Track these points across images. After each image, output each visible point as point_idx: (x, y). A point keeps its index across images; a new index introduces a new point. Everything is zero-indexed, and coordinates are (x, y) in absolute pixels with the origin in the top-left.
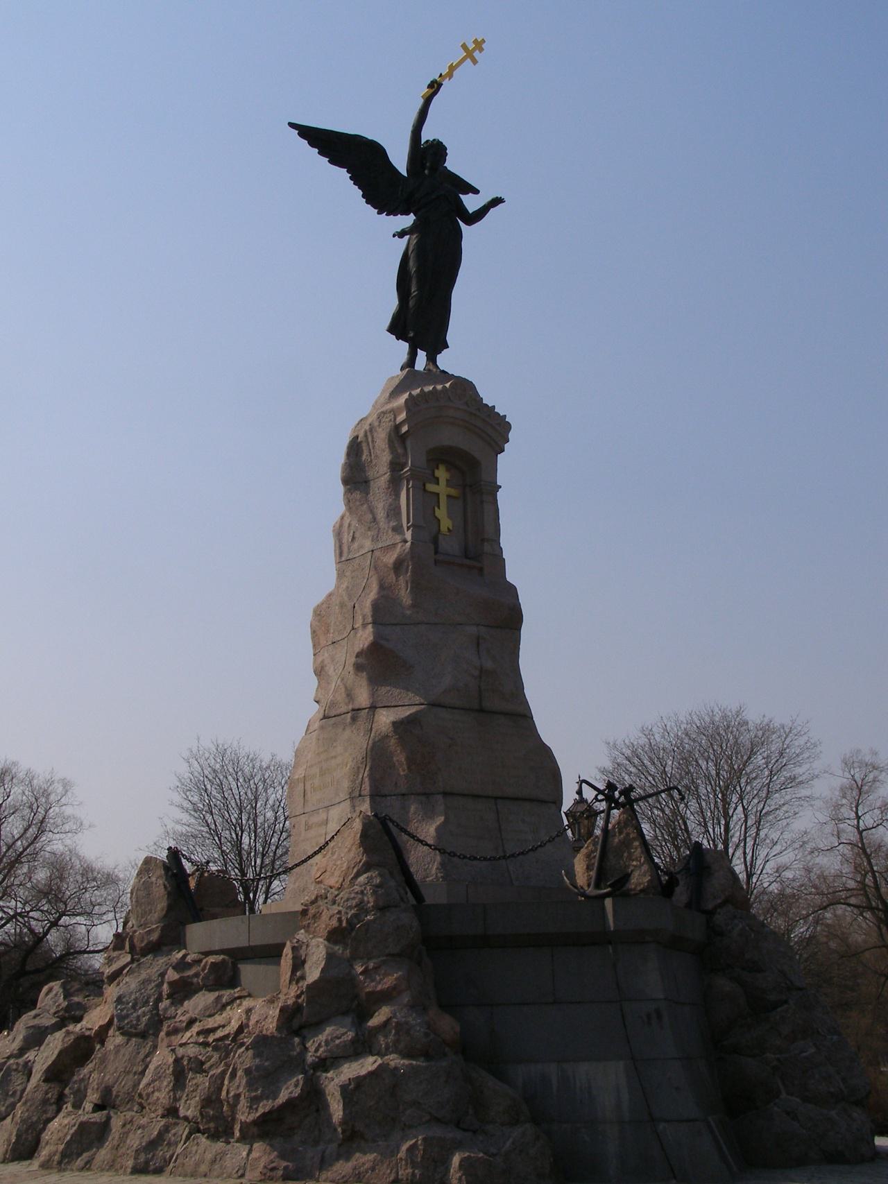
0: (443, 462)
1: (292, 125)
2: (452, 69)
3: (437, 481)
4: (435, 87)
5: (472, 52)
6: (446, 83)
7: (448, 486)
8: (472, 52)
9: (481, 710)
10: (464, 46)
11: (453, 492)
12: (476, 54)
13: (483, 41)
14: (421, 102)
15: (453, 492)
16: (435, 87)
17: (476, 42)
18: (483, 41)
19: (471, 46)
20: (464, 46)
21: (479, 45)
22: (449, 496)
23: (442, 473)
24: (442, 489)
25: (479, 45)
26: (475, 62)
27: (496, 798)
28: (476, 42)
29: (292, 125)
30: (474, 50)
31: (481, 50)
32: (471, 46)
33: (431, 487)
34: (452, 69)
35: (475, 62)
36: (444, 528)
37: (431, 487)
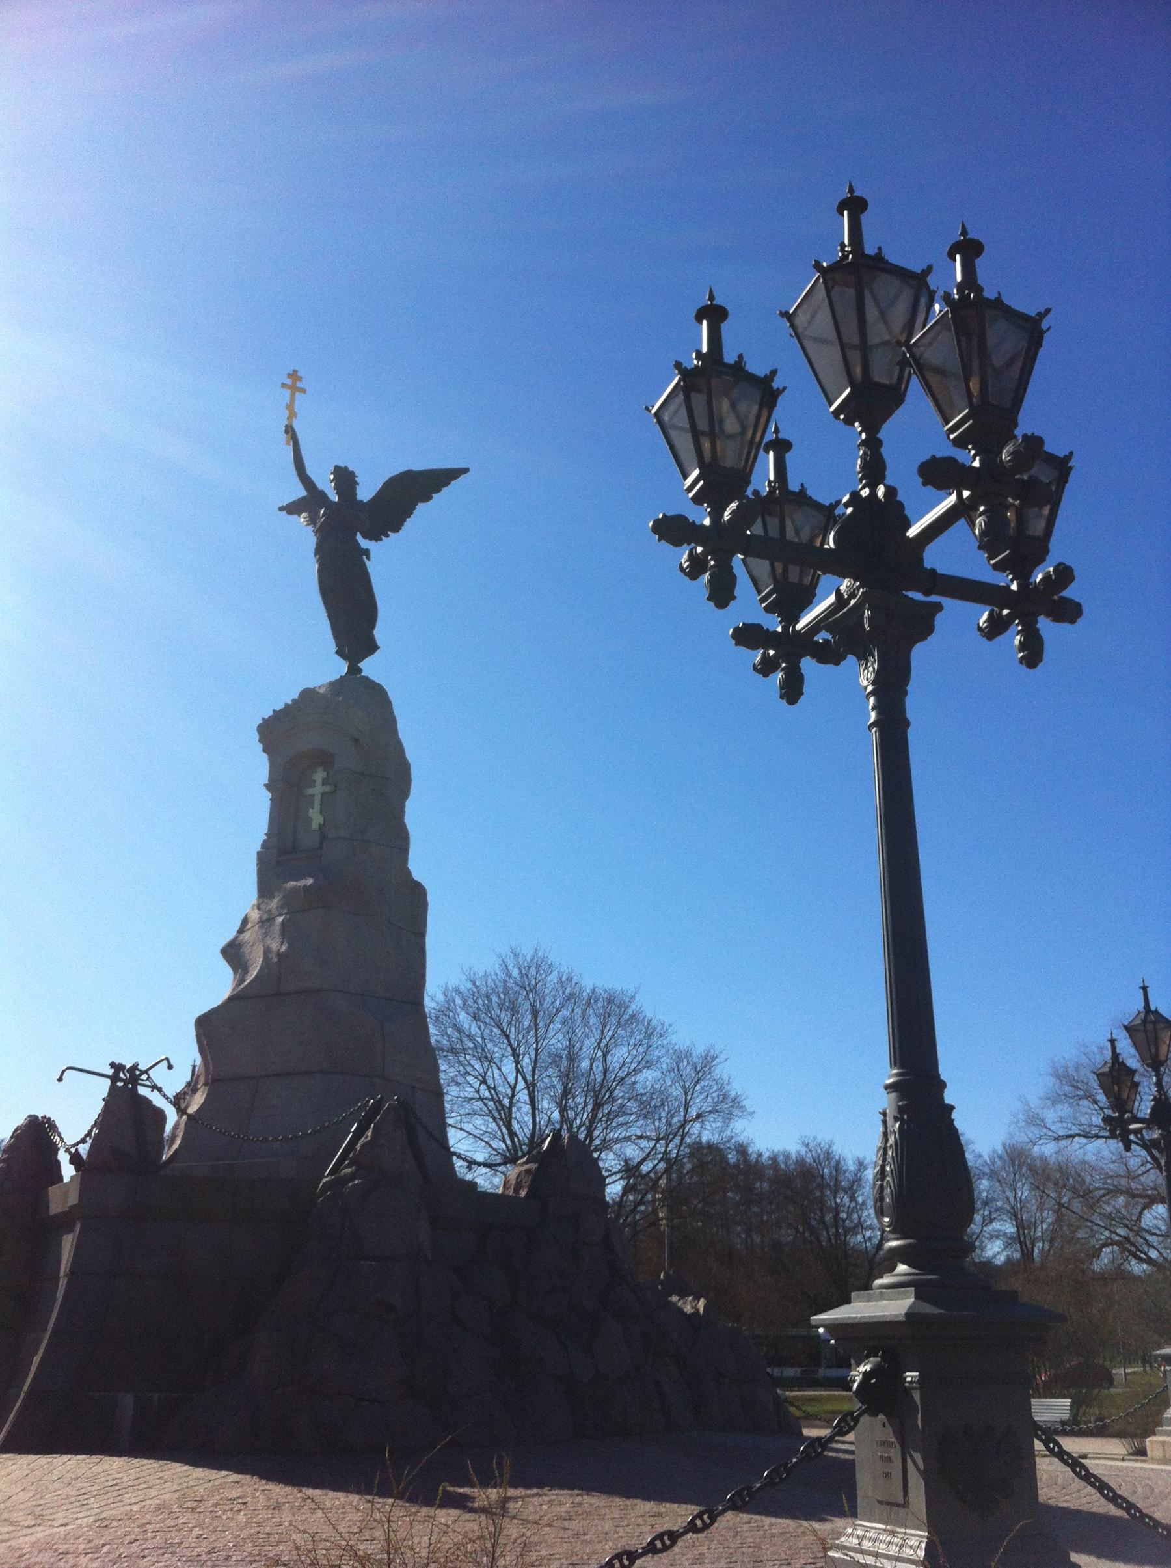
4: (290, 431)
10: (284, 385)
11: (327, 788)
12: (299, 385)
13: (295, 371)
16: (290, 431)
17: (289, 376)
20: (284, 385)
21: (294, 375)
22: (323, 794)
23: (319, 776)
24: (317, 789)
25: (294, 375)
26: (303, 391)
28: (289, 376)
30: (294, 384)
31: (300, 379)
32: (289, 382)
33: (310, 791)
34: (290, 407)
35: (303, 391)
37: (310, 791)
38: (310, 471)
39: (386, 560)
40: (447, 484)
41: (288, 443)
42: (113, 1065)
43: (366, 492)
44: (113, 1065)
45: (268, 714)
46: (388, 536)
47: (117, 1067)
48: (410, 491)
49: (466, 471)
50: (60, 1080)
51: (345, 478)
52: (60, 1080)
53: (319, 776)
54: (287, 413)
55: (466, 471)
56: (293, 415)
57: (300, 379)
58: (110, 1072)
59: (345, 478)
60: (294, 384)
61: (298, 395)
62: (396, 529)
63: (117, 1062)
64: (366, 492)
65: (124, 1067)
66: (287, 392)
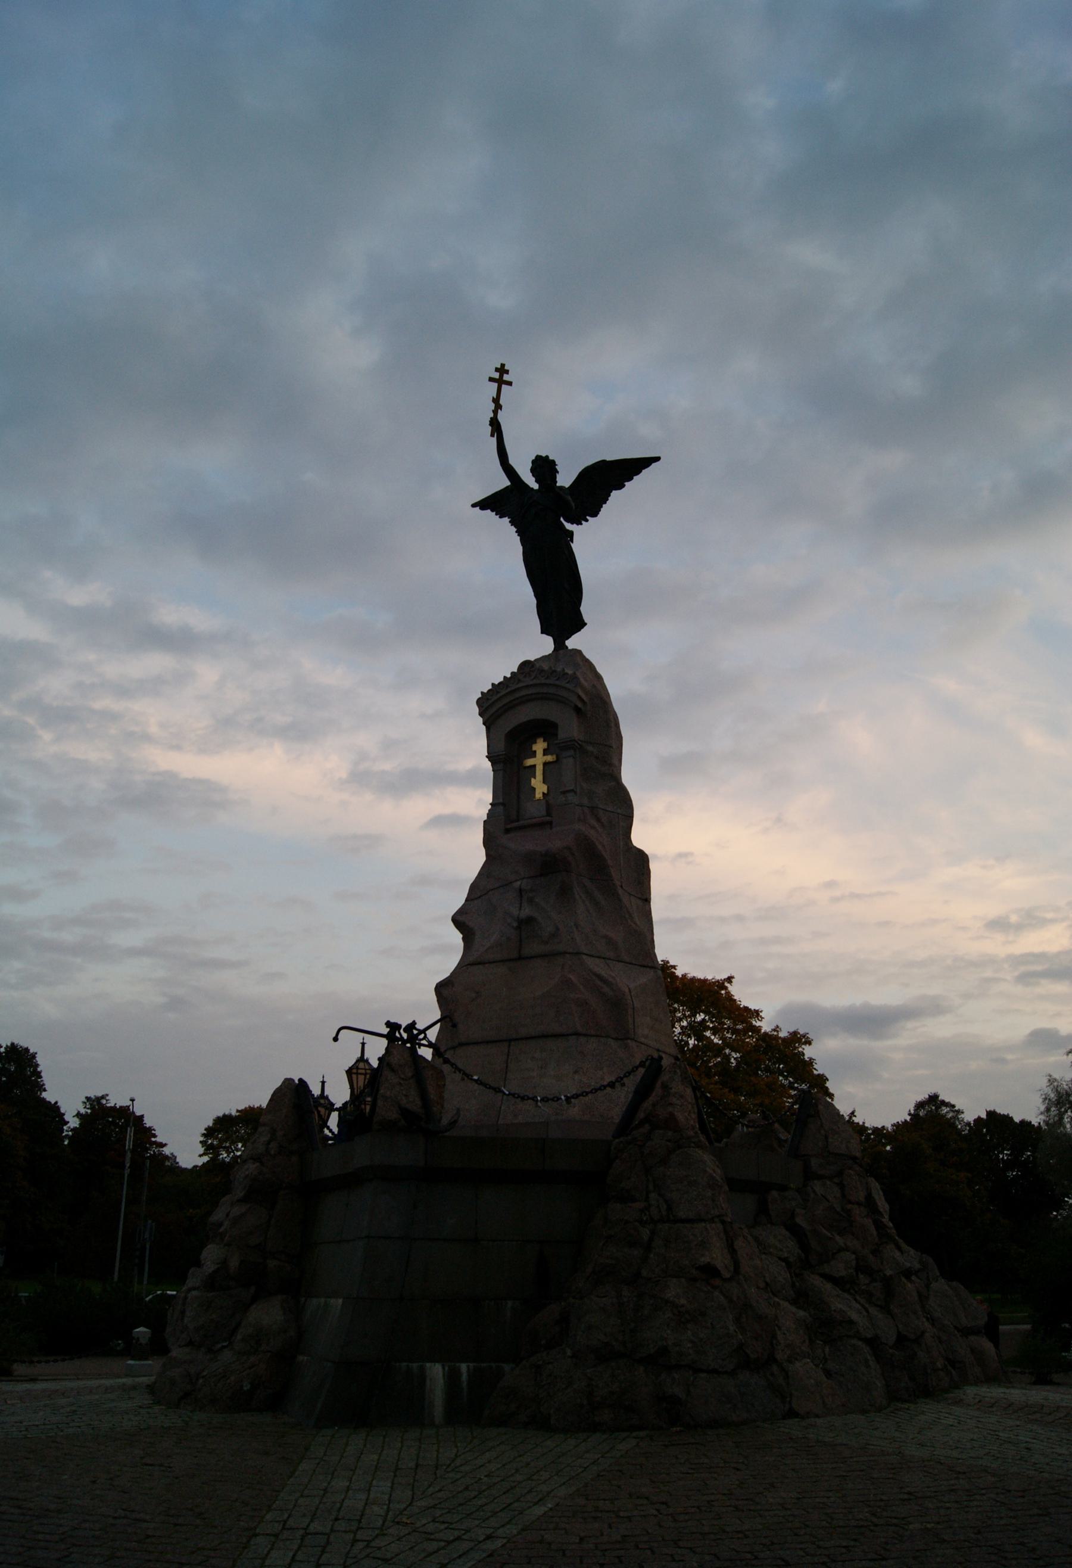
0: (539, 735)
1: (474, 506)
2: (496, 401)
3: (534, 754)
5: (501, 377)
6: (500, 414)
7: (544, 755)
8: (501, 377)
9: (520, 958)
10: (491, 379)
11: (549, 758)
12: (506, 377)
13: (503, 365)
14: (494, 439)
15: (549, 758)
17: (497, 370)
18: (503, 365)
19: (497, 375)
20: (491, 379)
21: (502, 370)
22: (545, 764)
23: (539, 746)
25: (502, 370)
26: (510, 383)
27: (510, 1041)
28: (497, 370)
29: (474, 506)
30: (501, 376)
31: (507, 372)
32: (497, 375)
33: (529, 762)
34: (496, 401)
35: (510, 383)
36: (539, 795)
37: (529, 762)
38: (512, 461)
39: (591, 543)
40: (638, 473)
41: (492, 435)
42: (388, 1024)
43: (565, 479)
44: (388, 1024)
45: (487, 687)
46: (587, 521)
47: (393, 1027)
48: (607, 478)
49: (657, 459)
50: (336, 1039)
51: (544, 467)
52: (336, 1039)
53: (539, 746)
54: (492, 406)
55: (657, 459)
56: (498, 406)
57: (507, 372)
58: (385, 1031)
59: (544, 467)
60: (501, 376)
61: (504, 386)
62: (595, 514)
63: (392, 1021)
64: (565, 479)
65: (400, 1026)
66: (496, 385)
